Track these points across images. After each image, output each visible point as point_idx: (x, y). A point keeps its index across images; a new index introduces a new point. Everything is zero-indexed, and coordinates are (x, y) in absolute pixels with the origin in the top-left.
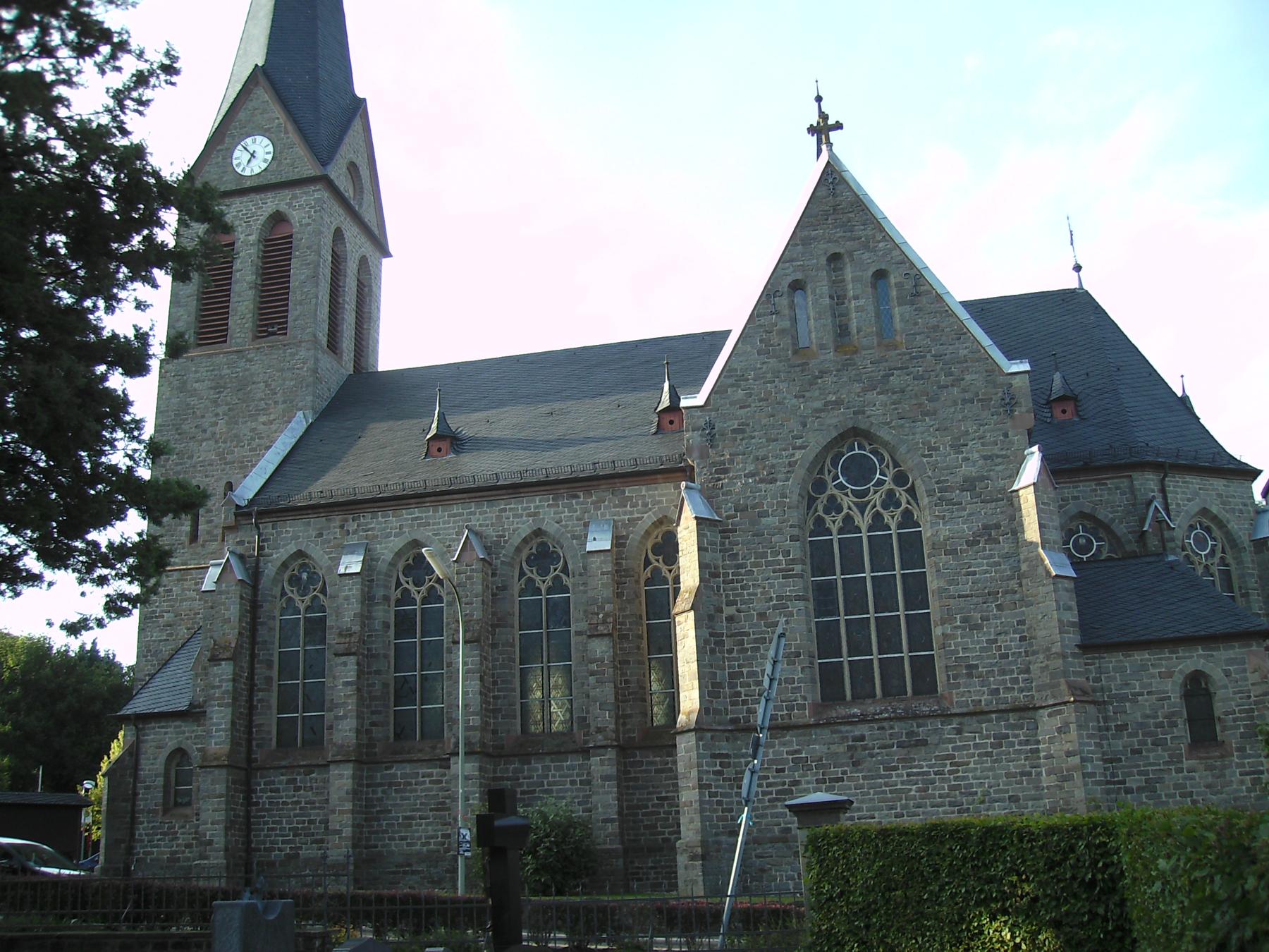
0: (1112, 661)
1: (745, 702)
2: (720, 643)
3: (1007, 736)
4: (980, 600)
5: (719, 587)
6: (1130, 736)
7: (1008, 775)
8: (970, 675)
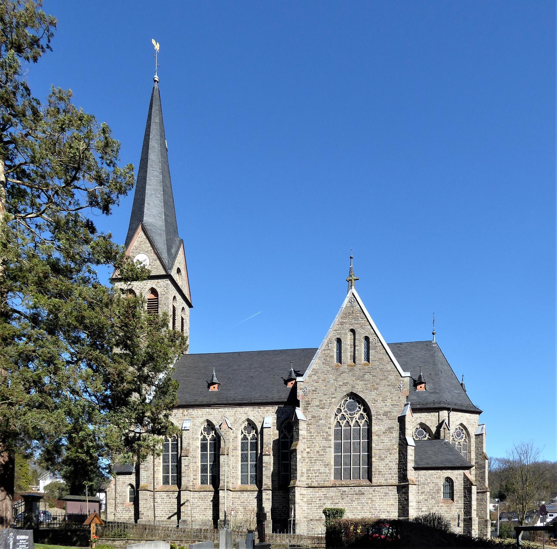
1: (311, 479)
2: (304, 460)
6: (425, 495)
7: (387, 505)
8: (379, 474)
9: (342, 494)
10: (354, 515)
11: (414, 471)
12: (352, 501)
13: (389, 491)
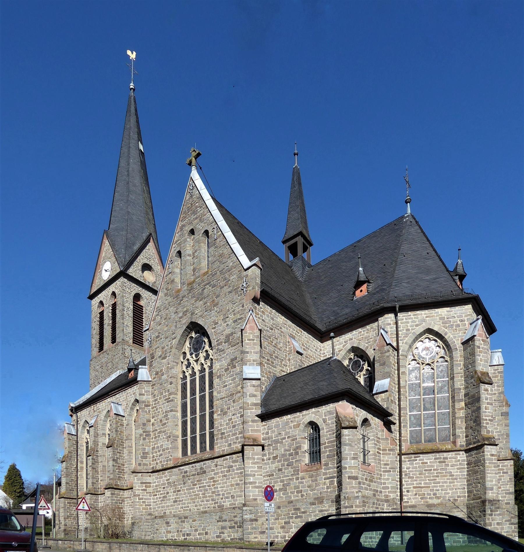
0: (274, 422)
2: (148, 435)
3: (232, 467)
4: (227, 399)
5: (149, 411)
6: (278, 462)
8: (222, 438)
9: (183, 476)
10: (196, 506)
11: (260, 423)
12: (194, 485)
13: (233, 462)
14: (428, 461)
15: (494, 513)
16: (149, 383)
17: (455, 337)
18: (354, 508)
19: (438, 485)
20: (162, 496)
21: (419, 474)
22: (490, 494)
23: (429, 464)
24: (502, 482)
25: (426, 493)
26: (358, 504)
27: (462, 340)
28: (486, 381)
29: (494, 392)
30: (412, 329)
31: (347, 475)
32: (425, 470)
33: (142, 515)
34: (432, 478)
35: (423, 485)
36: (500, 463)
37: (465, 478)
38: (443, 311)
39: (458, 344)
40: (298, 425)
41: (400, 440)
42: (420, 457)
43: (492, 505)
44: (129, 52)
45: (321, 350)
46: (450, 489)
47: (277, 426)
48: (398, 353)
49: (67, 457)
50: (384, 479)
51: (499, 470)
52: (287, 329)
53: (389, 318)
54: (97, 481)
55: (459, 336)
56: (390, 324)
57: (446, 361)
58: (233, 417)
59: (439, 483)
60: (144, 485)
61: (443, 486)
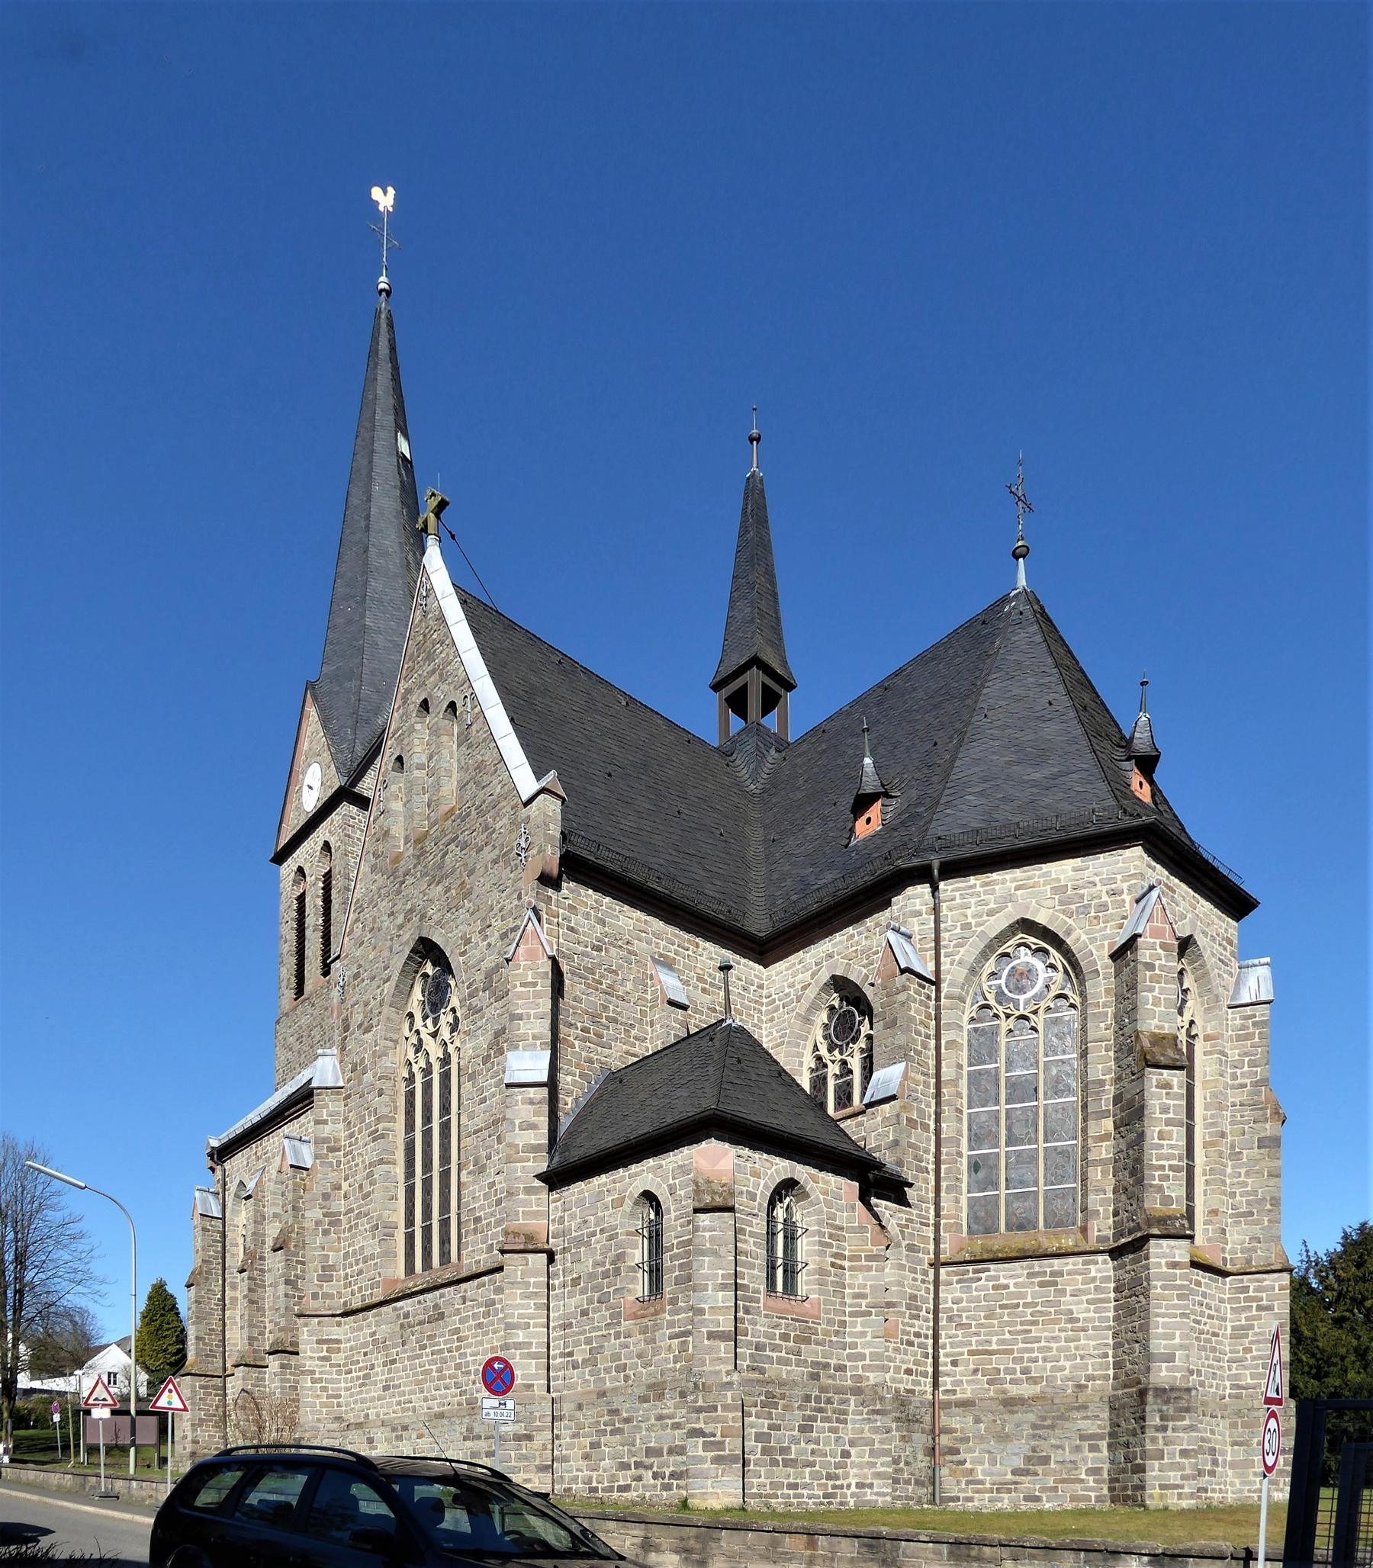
0: (578, 1190)
4: (486, 1133)
5: (339, 1163)
6: (582, 1292)
9: (402, 1326)
10: (425, 1400)
14: (1011, 1282)
15: (1170, 1424)
16: (338, 1093)
17: (1093, 940)
18: (719, 1412)
19: (1036, 1345)
20: (361, 1374)
21: (986, 1318)
22: (1164, 1373)
23: (1012, 1289)
24: (1256, 1334)
25: (1002, 1367)
26: (729, 1401)
27: (1111, 945)
28: (1163, 1060)
29: (1239, 1081)
30: (979, 925)
31: (704, 1330)
32: (1001, 1307)
33: (319, 1420)
34: (1019, 1328)
35: (994, 1347)
36: (1250, 1281)
37: (1109, 1328)
38: (1063, 870)
39: (1101, 958)
40: (620, 1202)
41: (937, 1226)
42: (988, 1270)
43: (1167, 1402)
44: (376, 193)
45: (761, 987)
46: (1067, 1358)
47: (580, 1203)
48: (938, 991)
49: (200, 1273)
50: (851, 1335)
51: (1246, 1300)
52: (649, 943)
53: (918, 895)
54: (262, 1334)
55: (1105, 937)
56: (918, 914)
57: (1072, 1006)
58: (497, 1178)
59: (1038, 1340)
60: (325, 1347)
61: (1050, 1349)
